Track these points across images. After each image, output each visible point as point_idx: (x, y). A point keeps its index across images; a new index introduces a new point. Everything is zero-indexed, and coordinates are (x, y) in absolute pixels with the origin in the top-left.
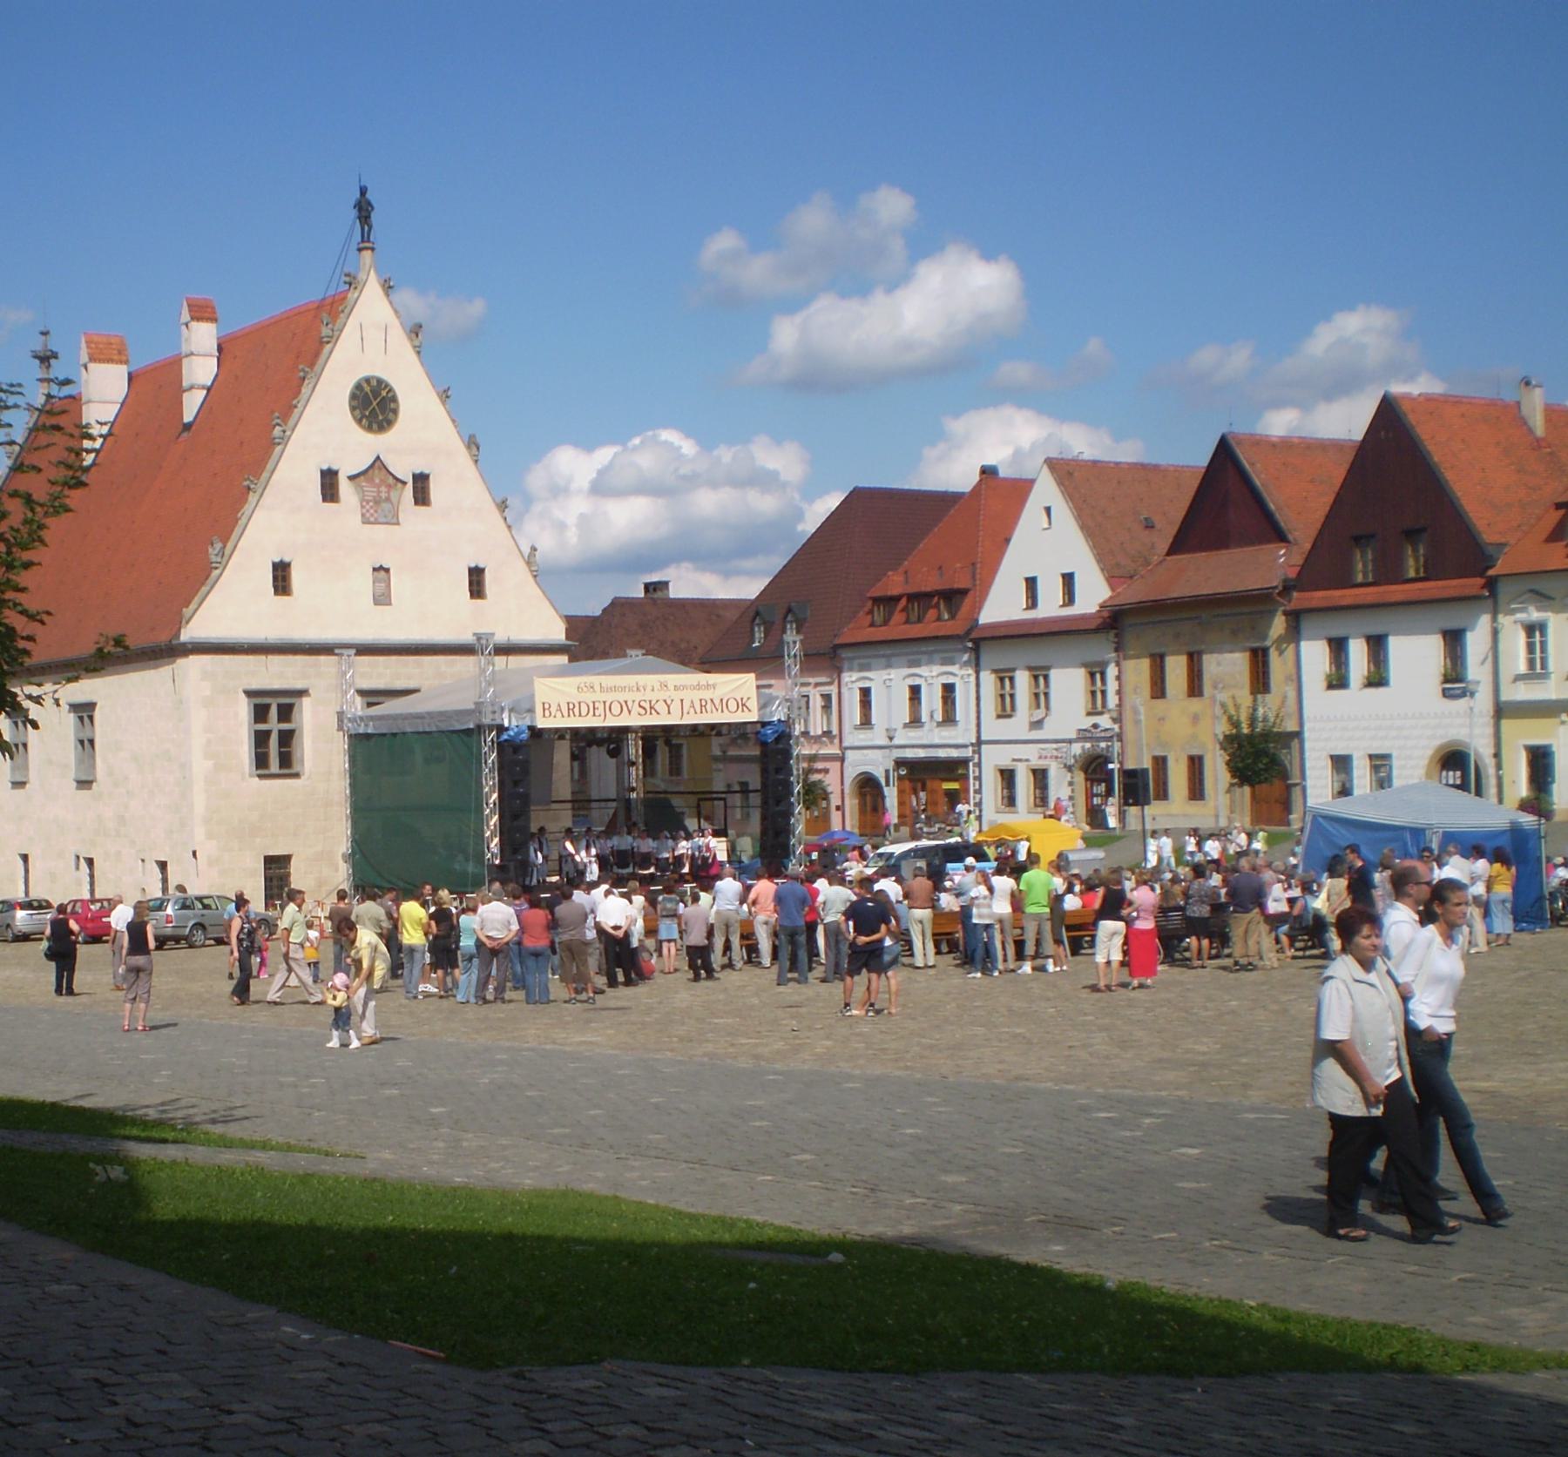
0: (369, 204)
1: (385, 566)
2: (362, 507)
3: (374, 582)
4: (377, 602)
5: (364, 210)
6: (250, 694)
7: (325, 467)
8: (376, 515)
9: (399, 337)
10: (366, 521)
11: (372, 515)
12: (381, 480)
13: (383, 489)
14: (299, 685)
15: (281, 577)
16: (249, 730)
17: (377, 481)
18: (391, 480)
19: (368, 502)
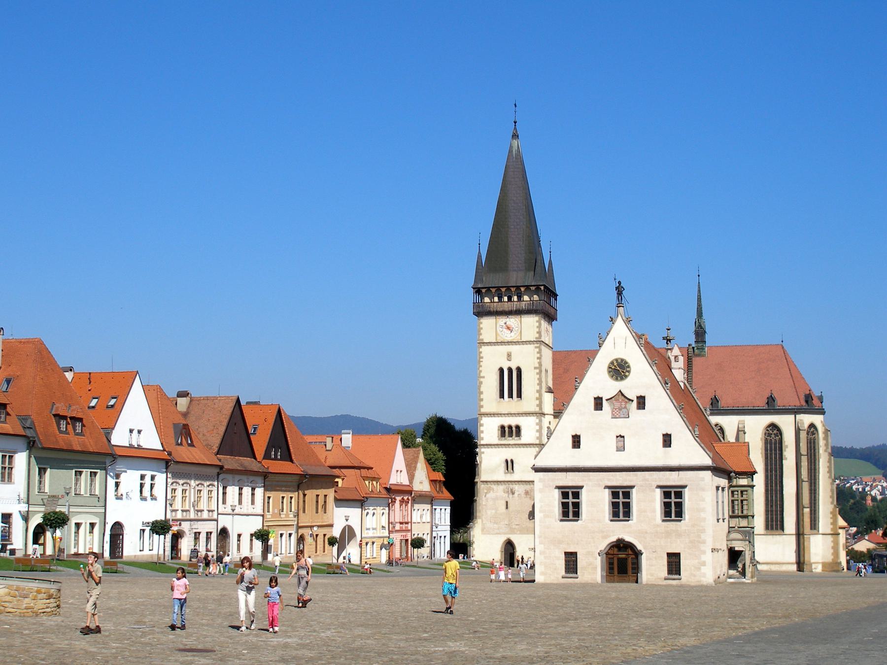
0: (622, 287)
1: (622, 435)
2: (613, 411)
3: (617, 442)
4: (618, 450)
5: (620, 290)
6: (559, 487)
7: (596, 396)
8: (619, 414)
9: (632, 341)
10: (614, 417)
11: (617, 414)
12: (622, 400)
13: (623, 403)
14: (580, 484)
15: (576, 441)
16: (684, 500)
17: (620, 400)
18: (627, 400)
19: (616, 409)
